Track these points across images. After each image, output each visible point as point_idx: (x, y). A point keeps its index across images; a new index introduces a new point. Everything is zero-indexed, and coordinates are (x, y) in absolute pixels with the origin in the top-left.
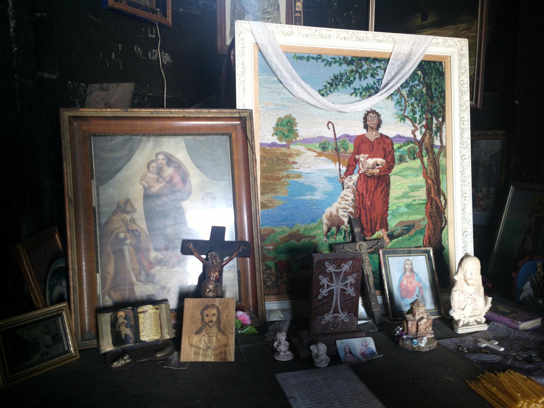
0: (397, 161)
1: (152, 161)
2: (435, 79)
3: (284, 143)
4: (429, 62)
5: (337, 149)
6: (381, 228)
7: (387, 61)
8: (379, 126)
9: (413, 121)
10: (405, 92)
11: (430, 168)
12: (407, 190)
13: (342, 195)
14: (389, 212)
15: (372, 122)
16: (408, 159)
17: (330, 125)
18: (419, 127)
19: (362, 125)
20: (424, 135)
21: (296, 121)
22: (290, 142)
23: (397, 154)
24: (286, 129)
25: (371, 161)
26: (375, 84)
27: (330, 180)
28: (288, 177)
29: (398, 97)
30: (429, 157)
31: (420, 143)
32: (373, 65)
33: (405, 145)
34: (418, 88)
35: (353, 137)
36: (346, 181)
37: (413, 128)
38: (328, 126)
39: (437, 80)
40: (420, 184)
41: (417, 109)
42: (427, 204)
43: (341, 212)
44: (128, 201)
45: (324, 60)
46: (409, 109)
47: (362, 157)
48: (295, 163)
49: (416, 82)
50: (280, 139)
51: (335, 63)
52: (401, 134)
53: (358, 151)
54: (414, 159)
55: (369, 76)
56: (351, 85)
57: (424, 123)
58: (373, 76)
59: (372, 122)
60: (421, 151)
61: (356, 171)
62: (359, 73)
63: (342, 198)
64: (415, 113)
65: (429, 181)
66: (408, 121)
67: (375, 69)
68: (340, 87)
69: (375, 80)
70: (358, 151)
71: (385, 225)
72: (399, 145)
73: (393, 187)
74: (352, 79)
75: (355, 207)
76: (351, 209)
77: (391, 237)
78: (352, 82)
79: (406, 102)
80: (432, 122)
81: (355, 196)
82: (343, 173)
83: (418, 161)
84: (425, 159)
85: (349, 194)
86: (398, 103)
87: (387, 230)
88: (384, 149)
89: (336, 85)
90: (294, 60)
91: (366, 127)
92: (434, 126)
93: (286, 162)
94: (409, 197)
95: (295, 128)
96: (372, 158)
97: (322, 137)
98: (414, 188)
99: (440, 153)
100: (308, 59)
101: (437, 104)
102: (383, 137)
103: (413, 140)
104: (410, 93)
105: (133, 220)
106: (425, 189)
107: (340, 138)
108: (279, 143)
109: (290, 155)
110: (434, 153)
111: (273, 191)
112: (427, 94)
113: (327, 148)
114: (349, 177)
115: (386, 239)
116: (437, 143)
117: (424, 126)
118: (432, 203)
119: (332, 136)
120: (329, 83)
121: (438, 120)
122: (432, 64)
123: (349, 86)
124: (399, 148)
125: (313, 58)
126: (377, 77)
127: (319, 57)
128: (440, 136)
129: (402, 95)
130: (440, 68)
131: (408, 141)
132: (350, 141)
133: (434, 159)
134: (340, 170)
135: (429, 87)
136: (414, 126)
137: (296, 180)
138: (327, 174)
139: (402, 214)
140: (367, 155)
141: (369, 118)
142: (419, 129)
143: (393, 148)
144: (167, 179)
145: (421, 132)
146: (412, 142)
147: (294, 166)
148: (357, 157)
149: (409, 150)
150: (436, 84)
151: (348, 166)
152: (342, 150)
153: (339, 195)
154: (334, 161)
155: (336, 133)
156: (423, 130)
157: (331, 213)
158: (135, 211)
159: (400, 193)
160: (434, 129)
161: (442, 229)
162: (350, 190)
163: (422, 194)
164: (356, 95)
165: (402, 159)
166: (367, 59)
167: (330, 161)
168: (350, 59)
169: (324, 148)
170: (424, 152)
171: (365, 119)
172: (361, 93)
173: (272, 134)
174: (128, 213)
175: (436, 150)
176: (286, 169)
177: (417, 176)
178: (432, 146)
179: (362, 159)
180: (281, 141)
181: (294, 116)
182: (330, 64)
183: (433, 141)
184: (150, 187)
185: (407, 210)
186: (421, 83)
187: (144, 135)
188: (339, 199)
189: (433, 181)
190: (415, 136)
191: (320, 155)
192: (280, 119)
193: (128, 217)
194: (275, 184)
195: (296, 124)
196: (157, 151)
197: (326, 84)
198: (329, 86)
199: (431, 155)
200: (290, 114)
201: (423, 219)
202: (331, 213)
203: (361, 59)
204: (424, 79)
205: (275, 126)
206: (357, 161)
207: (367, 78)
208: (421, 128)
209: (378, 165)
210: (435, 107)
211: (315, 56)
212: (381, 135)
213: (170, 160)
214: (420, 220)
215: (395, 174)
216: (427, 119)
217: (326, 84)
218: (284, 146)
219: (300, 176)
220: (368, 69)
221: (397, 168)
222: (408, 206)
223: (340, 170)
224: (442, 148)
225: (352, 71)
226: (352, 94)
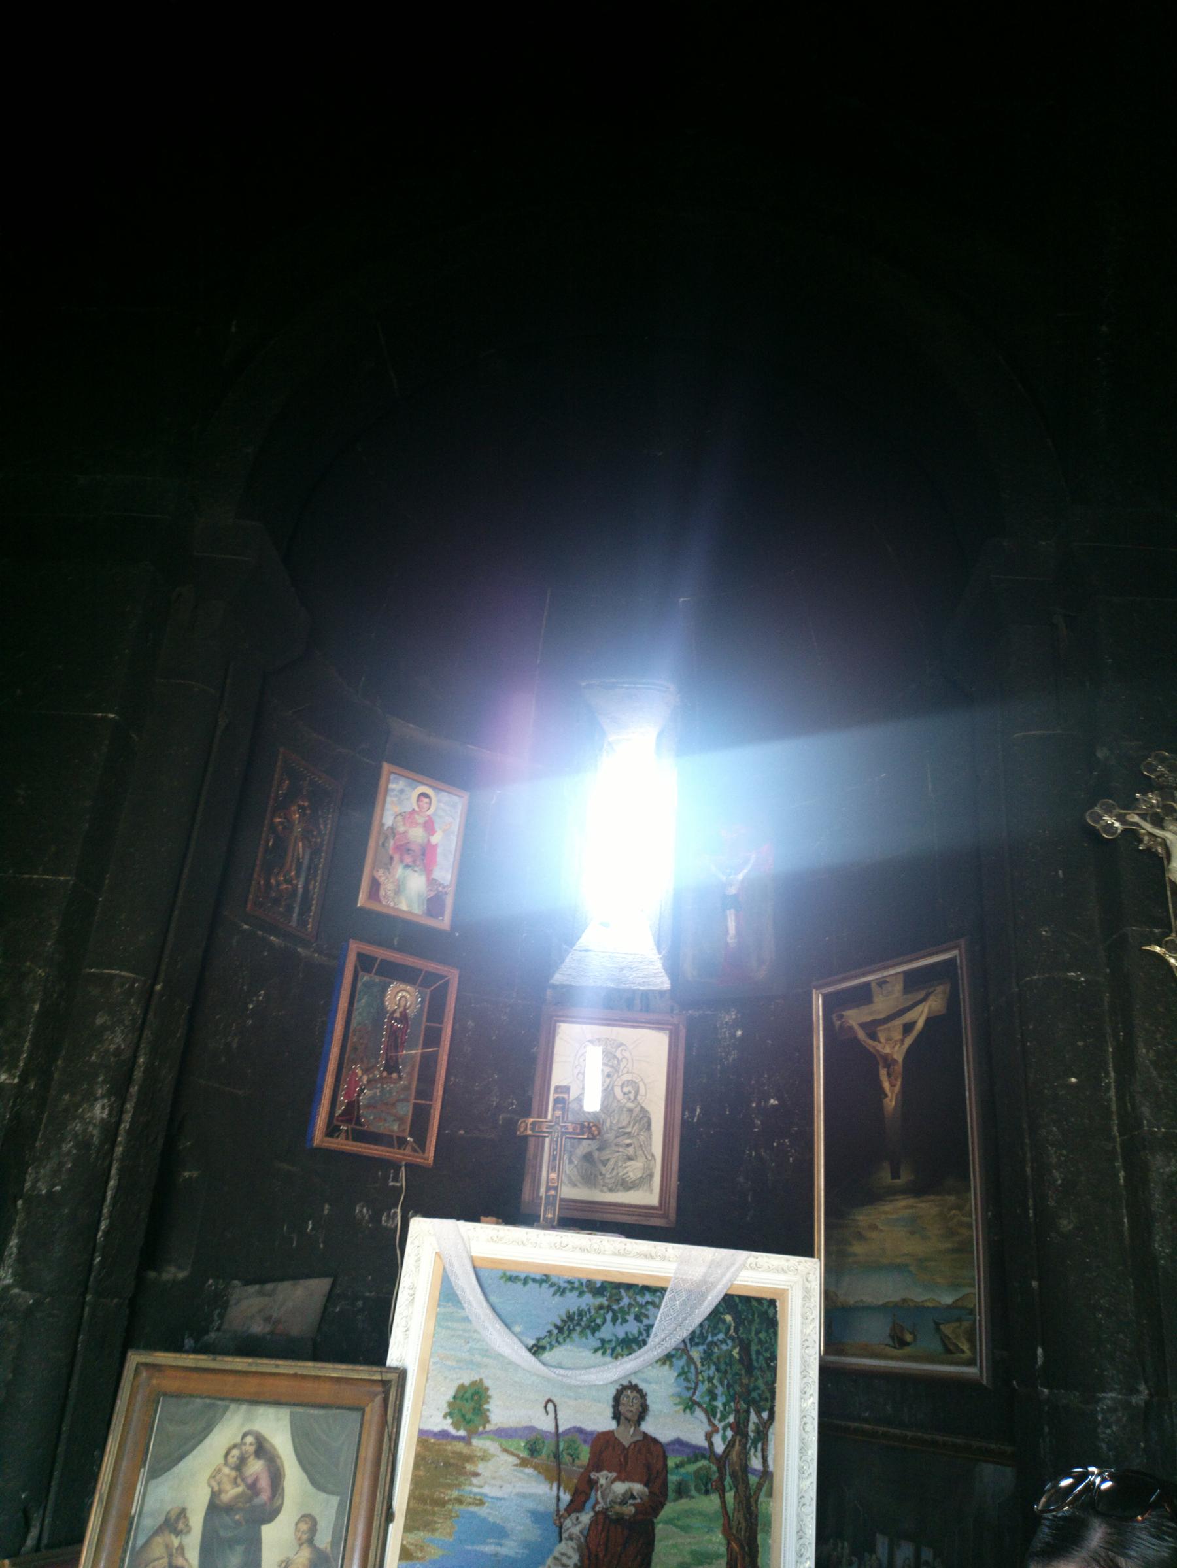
0: (671, 1494)
1: (235, 1446)
2: (757, 1333)
3: (462, 1433)
4: (747, 1300)
5: (557, 1456)
7: (663, 1290)
9: (710, 1413)
10: (696, 1353)
11: (737, 1517)
12: (688, 1559)
16: (693, 1492)
17: (550, 1406)
18: (720, 1426)
19: (609, 1412)
20: (730, 1446)
21: (490, 1393)
22: (472, 1433)
23: (673, 1478)
24: (469, 1405)
25: (620, 1488)
26: (640, 1333)
27: (537, 1517)
28: (459, 1501)
29: (683, 1362)
30: (737, 1492)
32: (640, 1299)
33: (689, 1462)
34: (724, 1347)
35: (591, 1433)
36: (568, 1523)
37: (709, 1429)
38: (546, 1407)
39: (762, 1336)
40: (711, 1548)
41: (719, 1390)
44: (182, 1513)
45: (552, 1285)
46: (704, 1387)
48: (476, 1475)
49: (721, 1336)
50: (456, 1425)
51: (572, 1289)
52: (685, 1437)
54: (707, 1492)
55: (631, 1318)
56: (597, 1334)
57: (731, 1419)
58: (638, 1318)
59: (630, 1406)
60: (722, 1479)
61: (589, 1505)
62: (614, 1312)
63: (556, 1559)
64: (713, 1396)
65: (734, 1545)
66: (699, 1413)
67: (641, 1306)
68: (575, 1335)
69: (642, 1327)
70: (597, 1464)
72: (678, 1460)
73: (659, 1547)
74: (599, 1321)
78: (598, 1327)
79: (697, 1373)
80: (748, 1420)
81: (581, 1560)
82: (563, 1505)
83: (715, 1498)
84: (730, 1496)
85: (571, 1552)
86: (683, 1373)
88: (648, 1467)
89: (570, 1331)
90: (502, 1281)
91: (617, 1416)
92: (751, 1427)
93: (461, 1471)
95: (485, 1407)
96: (623, 1481)
97: (532, 1429)
99: (760, 1486)
101: (760, 1383)
102: (649, 1441)
104: (707, 1357)
105: (181, 1549)
108: (453, 1431)
109: (469, 1458)
111: (428, 1526)
112: (741, 1361)
113: (539, 1452)
114: (574, 1516)
116: (756, 1463)
117: (730, 1425)
119: (552, 1429)
120: (557, 1327)
122: (754, 1303)
123: (593, 1333)
124: (678, 1466)
125: (534, 1280)
126: (646, 1322)
127: (545, 1280)
128: (764, 1451)
129: (691, 1360)
130: (771, 1311)
131: (697, 1453)
132: (585, 1442)
133: (748, 1498)
134: (558, 1499)
135: (745, 1347)
137: (473, 1509)
140: (614, 1475)
141: (624, 1400)
142: (721, 1432)
143: (665, 1465)
144: (250, 1481)
145: (724, 1438)
146: (704, 1457)
147: (475, 1480)
148: (594, 1475)
149: (697, 1472)
150: (760, 1342)
151: (576, 1494)
152: (566, 1459)
153: (551, 1551)
154: (550, 1480)
155: (560, 1423)
156: (729, 1433)
158: (189, 1530)
160: (752, 1434)
162: (573, 1544)
164: (604, 1353)
166: (629, 1287)
167: (542, 1478)
168: (598, 1285)
169: (533, 1450)
170: (728, 1481)
171: (617, 1400)
172: (613, 1349)
173: (443, 1413)
174: (178, 1533)
175: (753, 1480)
176: (458, 1486)
177: (710, 1530)
178: (745, 1468)
179: (602, 1481)
180: (458, 1430)
181: (488, 1383)
182: (561, 1291)
184: (220, 1491)
186: (732, 1338)
187: (234, 1400)
189: (741, 1547)
190: (711, 1444)
191: (524, 1463)
192: (462, 1388)
193: (176, 1542)
194: (434, 1514)
195: (487, 1399)
196: (246, 1429)
197: (551, 1327)
198: (555, 1331)
199: (741, 1487)
200: (481, 1380)
203: (618, 1286)
204: (736, 1330)
205: (451, 1400)
206: (592, 1484)
207: (625, 1321)
208: (724, 1429)
209: (633, 1497)
210: (756, 1388)
211: (538, 1277)
212: (645, 1435)
213: (262, 1449)
215: (669, 1522)
216: (737, 1411)
217: (551, 1327)
219: (481, 1503)
220: (630, 1305)
221: (670, 1509)
223: (558, 1499)
224: (766, 1475)
225: (601, 1307)
226: (596, 1350)
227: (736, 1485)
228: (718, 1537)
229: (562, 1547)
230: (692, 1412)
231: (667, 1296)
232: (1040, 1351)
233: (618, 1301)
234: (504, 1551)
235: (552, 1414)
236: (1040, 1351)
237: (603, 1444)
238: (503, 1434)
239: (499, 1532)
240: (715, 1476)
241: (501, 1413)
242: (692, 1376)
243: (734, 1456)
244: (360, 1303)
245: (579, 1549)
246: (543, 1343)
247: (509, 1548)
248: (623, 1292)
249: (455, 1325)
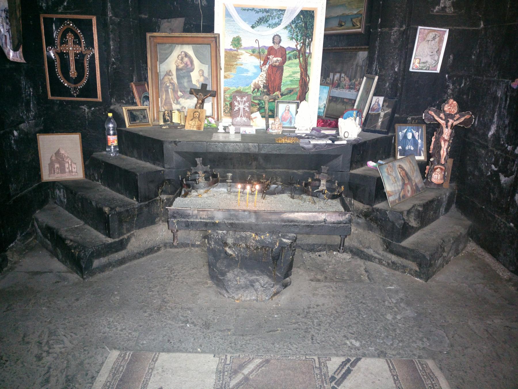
1: (180, 55)
2: (309, 19)
3: (235, 49)
4: (307, 11)
5: (259, 53)
6: (277, 91)
7: (285, 10)
9: (297, 40)
10: (293, 26)
11: (303, 63)
12: (291, 73)
13: (261, 74)
14: (282, 83)
15: (277, 40)
16: (293, 59)
17: (257, 41)
18: (299, 43)
20: (302, 47)
22: (238, 49)
23: (288, 56)
24: (236, 43)
25: (275, 59)
26: (279, 22)
27: (256, 67)
29: (290, 28)
31: (299, 51)
32: (278, 13)
33: (292, 52)
34: (300, 24)
35: (267, 47)
36: (263, 68)
37: (296, 44)
39: (310, 20)
40: (297, 71)
41: (299, 34)
42: (300, 80)
43: (260, 82)
44: (170, 71)
45: (255, 11)
46: (295, 34)
48: (240, 58)
49: (300, 21)
50: (234, 47)
51: (260, 12)
52: (290, 46)
53: (269, 54)
54: (296, 58)
55: (276, 18)
57: (302, 41)
58: (278, 18)
59: (277, 40)
60: (299, 55)
61: (268, 63)
62: (272, 17)
64: (297, 36)
65: (302, 70)
66: (294, 40)
67: (279, 15)
68: (262, 23)
70: (269, 54)
71: (279, 89)
73: (284, 71)
75: (266, 80)
76: (265, 81)
77: (282, 95)
78: (268, 21)
79: (294, 31)
83: (298, 60)
84: (301, 59)
85: (264, 74)
86: (290, 31)
87: (280, 92)
88: (282, 54)
89: (261, 22)
90: (242, 11)
91: (274, 42)
92: (307, 43)
93: (236, 58)
94: (292, 77)
97: (252, 47)
99: (308, 56)
100: (248, 10)
101: (309, 32)
102: (282, 48)
103: (296, 49)
105: (172, 79)
106: (299, 73)
107: (262, 47)
108: (233, 49)
109: (238, 55)
110: (305, 56)
111: (230, 71)
112: (305, 27)
113: (255, 52)
115: (280, 96)
116: (308, 51)
117: (302, 43)
118: (302, 80)
119: (258, 47)
120: (257, 21)
122: (309, 12)
124: (289, 53)
125: (250, 10)
126: (280, 19)
127: (253, 9)
128: (310, 48)
129: (292, 27)
130: (313, 14)
131: (294, 50)
133: (306, 59)
135: (306, 24)
137: (240, 66)
139: (288, 85)
141: (275, 38)
143: (286, 53)
144: (185, 63)
145: (300, 46)
146: (295, 51)
147: (240, 60)
148: (268, 57)
150: (310, 22)
151: (264, 61)
152: (262, 53)
156: (301, 45)
157: (255, 83)
158: (173, 75)
159: (288, 74)
161: (306, 93)
162: (264, 72)
163: (298, 76)
165: (290, 59)
169: (253, 52)
170: (301, 55)
171: (273, 39)
172: (272, 26)
174: (170, 76)
175: (307, 55)
176: (236, 61)
177: (296, 67)
178: (305, 52)
179: (271, 58)
181: (240, 36)
182: (257, 12)
183: (305, 50)
184: (178, 66)
185: (290, 83)
186: (302, 21)
187: (177, 44)
188: (259, 76)
190: (297, 47)
191: (251, 55)
192: (234, 38)
193: (170, 77)
194: (231, 68)
196: (182, 51)
197: (256, 22)
199: (304, 57)
201: (298, 88)
202: (255, 83)
206: (268, 59)
207: (275, 19)
208: (300, 44)
209: (278, 61)
210: (308, 33)
212: (281, 46)
213: (186, 55)
214: (296, 88)
215: (286, 66)
216: (303, 39)
217: (256, 22)
219: (242, 65)
220: (276, 15)
221: (287, 63)
222: (291, 81)
225: (268, 16)
226: (268, 27)
231: (286, 11)
232: (380, 19)
233: (273, 14)
234: (248, 75)
236: (380, 19)
237: (271, 50)
238: (245, 48)
240: (298, 55)
241: (245, 43)
242: (292, 31)
243: (302, 50)
244: (192, 25)
245: (266, 73)
246: (254, 26)
248: (274, 11)
249: (230, 22)
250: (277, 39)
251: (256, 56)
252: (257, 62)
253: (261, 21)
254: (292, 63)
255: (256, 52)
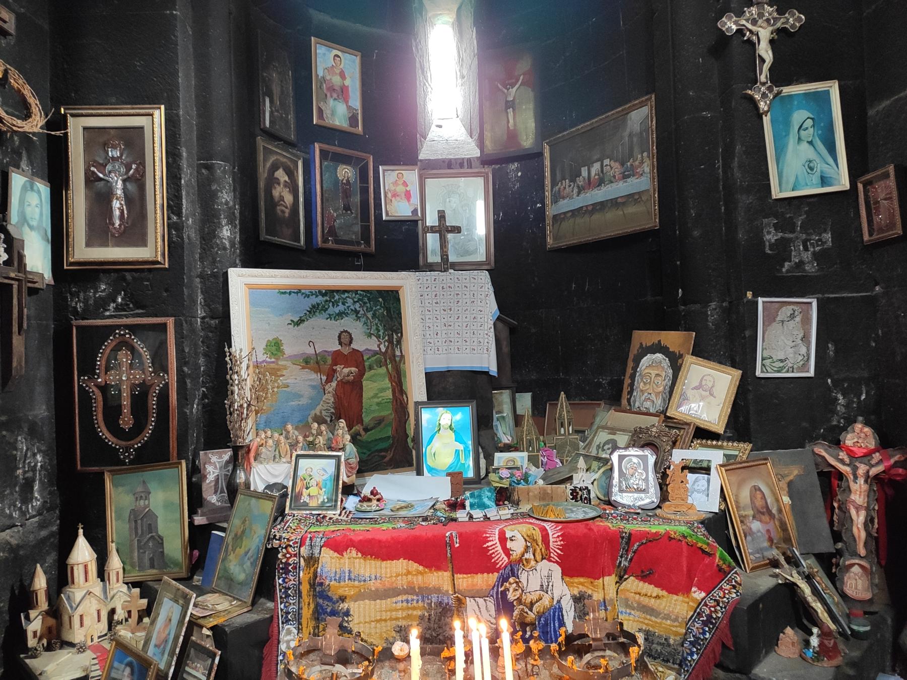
0: (367, 369)
3: (273, 360)
5: (317, 363)
8: (351, 342)
9: (378, 337)
11: (394, 374)
14: (364, 410)
17: (311, 343)
19: (337, 342)
20: (388, 348)
23: (367, 364)
24: (274, 348)
25: (346, 370)
27: (313, 387)
40: (385, 386)
41: (381, 328)
42: (393, 402)
43: (324, 413)
46: (374, 328)
47: (338, 368)
54: (381, 367)
55: (340, 304)
57: (387, 338)
58: (343, 304)
59: (347, 340)
60: (386, 361)
66: (373, 337)
67: (344, 299)
68: (317, 314)
71: (361, 421)
75: (335, 408)
76: (333, 410)
77: (366, 430)
78: (327, 309)
79: (371, 322)
81: (335, 399)
82: (323, 382)
84: (390, 366)
87: (362, 425)
89: (314, 312)
91: (340, 343)
92: (395, 340)
98: (383, 390)
99: (400, 361)
100: (290, 293)
101: (396, 323)
104: (374, 316)
106: (391, 390)
108: (268, 360)
109: (279, 370)
115: (362, 433)
116: (398, 353)
121: (397, 336)
124: (368, 359)
125: (294, 292)
126: (347, 305)
128: (400, 348)
129: (368, 318)
131: (375, 353)
135: (388, 310)
136: (379, 341)
138: (311, 383)
139: (374, 411)
141: (342, 337)
145: (385, 346)
146: (378, 354)
148: (335, 368)
153: (321, 399)
154: (316, 372)
156: (387, 344)
157: (316, 414)
163: (389, 394)
165: (371, 368)
166: (337, 291)
168: (324, 291)
171: (339, 337)
175: (398, 359)
178: (394, 356)
179: (338, 369)
183: (394, 352)
185: (377, 408)
188: (322, 403)
190: (380, 349)
191: (303, 368)
199: (394, 363)
201: (391, 414)
202: (316, 414)
203: (333, 291)
206: (335, 371)
207: (338, 305)
214: (388, 415)
218: (273, 362)
219: (288, 386)
221: (367, 375)
222: (378, 404)
224: (402, 356)
225: (327, 301)
226: (327, 319)
227: (391, 362)
228: (387, 381)
229: (326, 396)
230: (370, 337)
233: (334, 298)
235: (312, 347)
239: (298, 396)
240: (383, 360)
241: (288, 350)
242: (369, 324)
247: (304, 401)
250: (345, 338)
251: (311, 369)
252: (316, 378)
253: (314, 310)
254: (373, 376)
255: (312, 362)
